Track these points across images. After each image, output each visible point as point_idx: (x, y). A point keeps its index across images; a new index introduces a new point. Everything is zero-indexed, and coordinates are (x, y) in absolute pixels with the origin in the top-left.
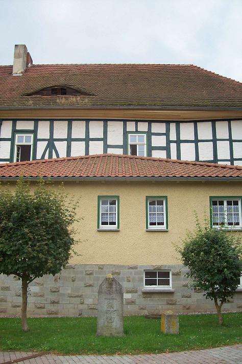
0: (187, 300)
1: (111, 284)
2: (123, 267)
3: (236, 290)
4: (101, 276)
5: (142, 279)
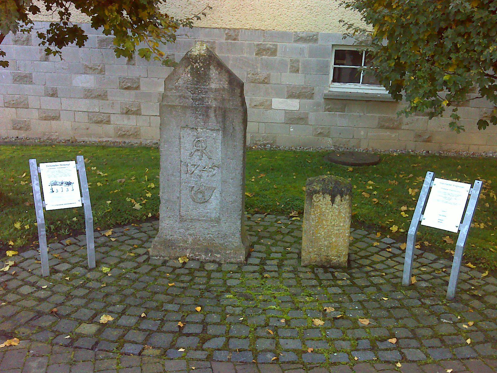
0: (38, 193)
1: (200, 77)
2: (284, 36)
3: (100, 269)
4: (231, 56)
5: (327, 66)
